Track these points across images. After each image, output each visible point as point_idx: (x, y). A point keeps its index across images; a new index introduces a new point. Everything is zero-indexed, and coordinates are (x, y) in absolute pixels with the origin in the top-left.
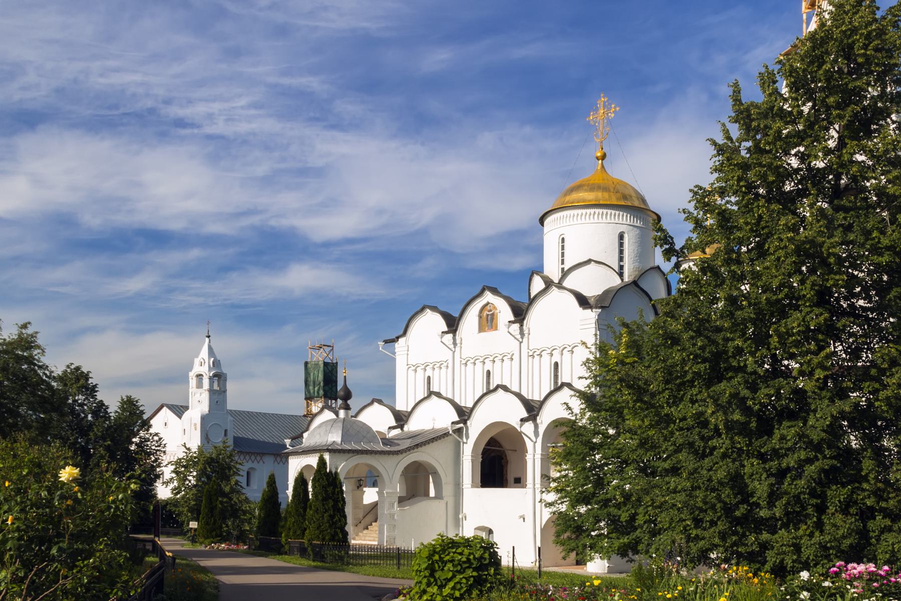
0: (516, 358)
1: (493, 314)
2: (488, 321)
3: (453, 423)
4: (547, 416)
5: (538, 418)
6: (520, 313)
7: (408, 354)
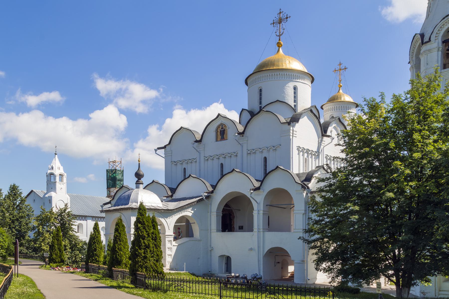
0: (239, 155)
1: (224, 130)
7: (171, 155)
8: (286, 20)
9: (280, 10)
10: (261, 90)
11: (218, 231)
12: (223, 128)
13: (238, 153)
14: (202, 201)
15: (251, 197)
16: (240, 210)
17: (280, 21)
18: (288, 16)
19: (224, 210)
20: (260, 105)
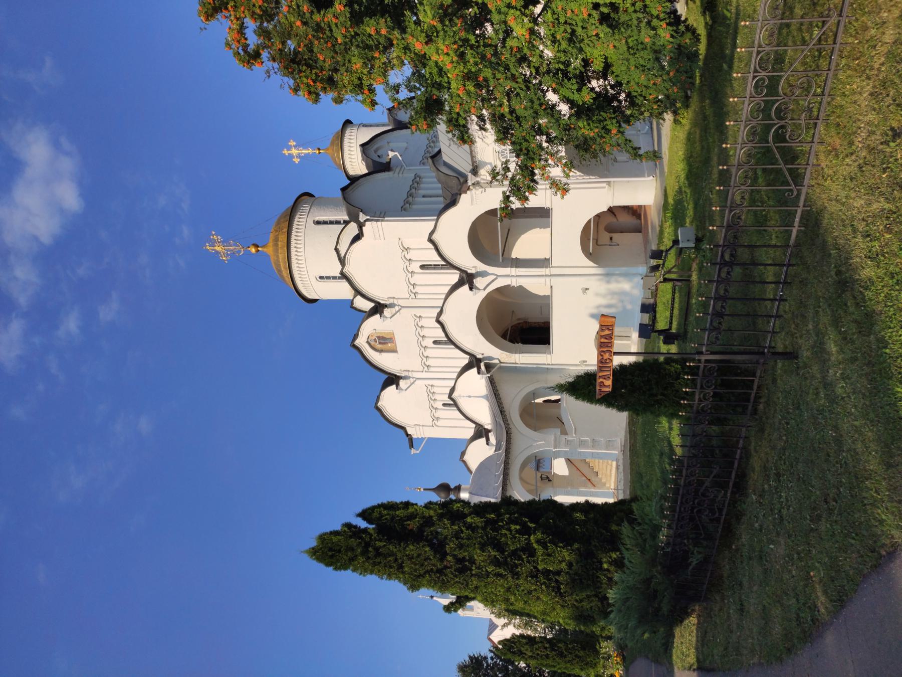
0: (419, 312)
1: (379, 337)
2: (384, 342)
3: (479, 373)
4: (471, 263)
5: (469, 271)
6: (378, 308)
10: (321, 278)
12: (375, 339)
13: (415, 315)
14: (493, 379)
15: (484, 289)
16: (513, 312)
19: (513, 340)
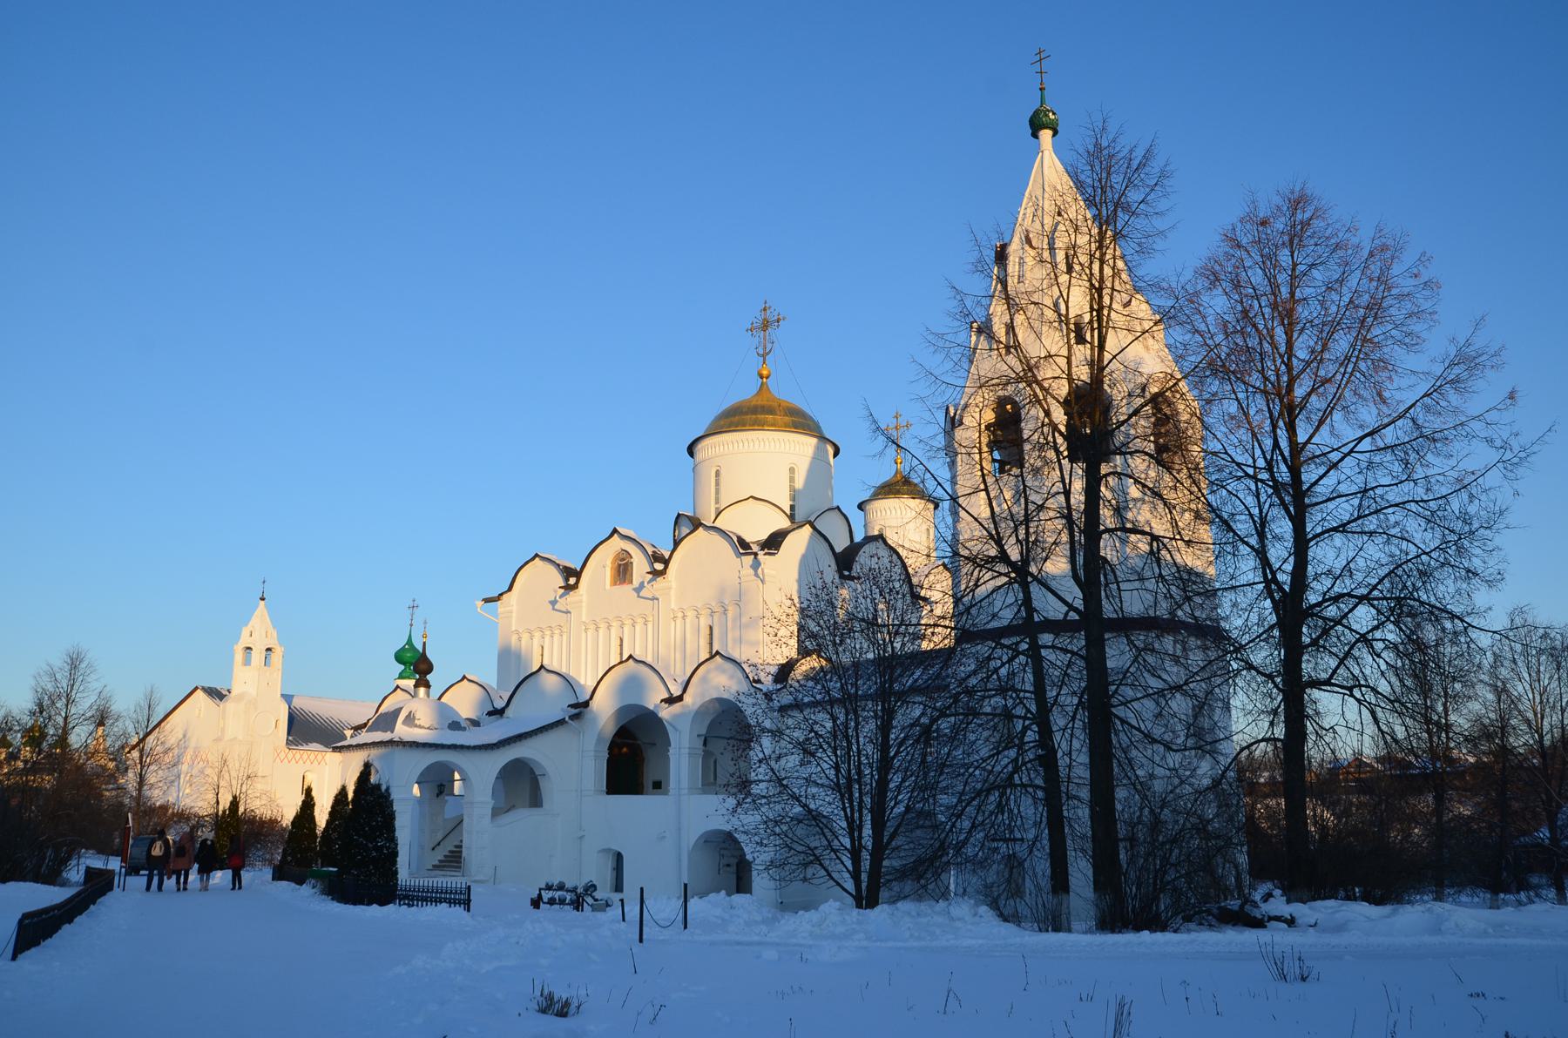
8: (776, 324)
9: (766, 303)
11: (692, 790)
16: (655, 744)
17: (765, 325)
18: (781, 317)
20: (717, 506)
